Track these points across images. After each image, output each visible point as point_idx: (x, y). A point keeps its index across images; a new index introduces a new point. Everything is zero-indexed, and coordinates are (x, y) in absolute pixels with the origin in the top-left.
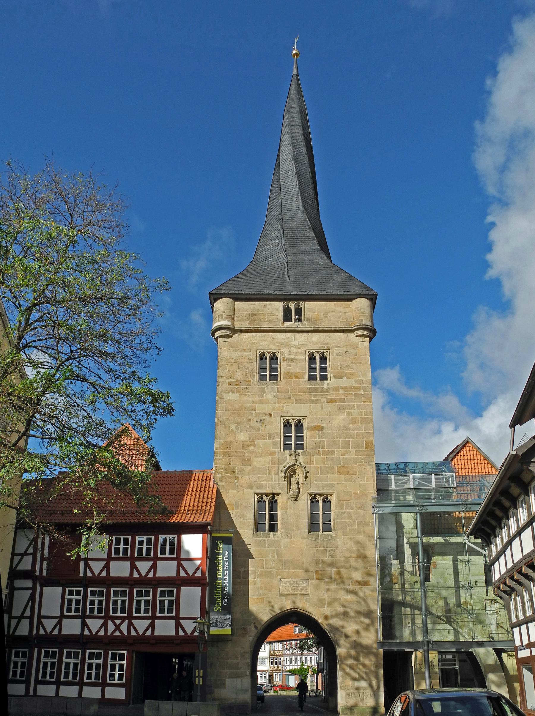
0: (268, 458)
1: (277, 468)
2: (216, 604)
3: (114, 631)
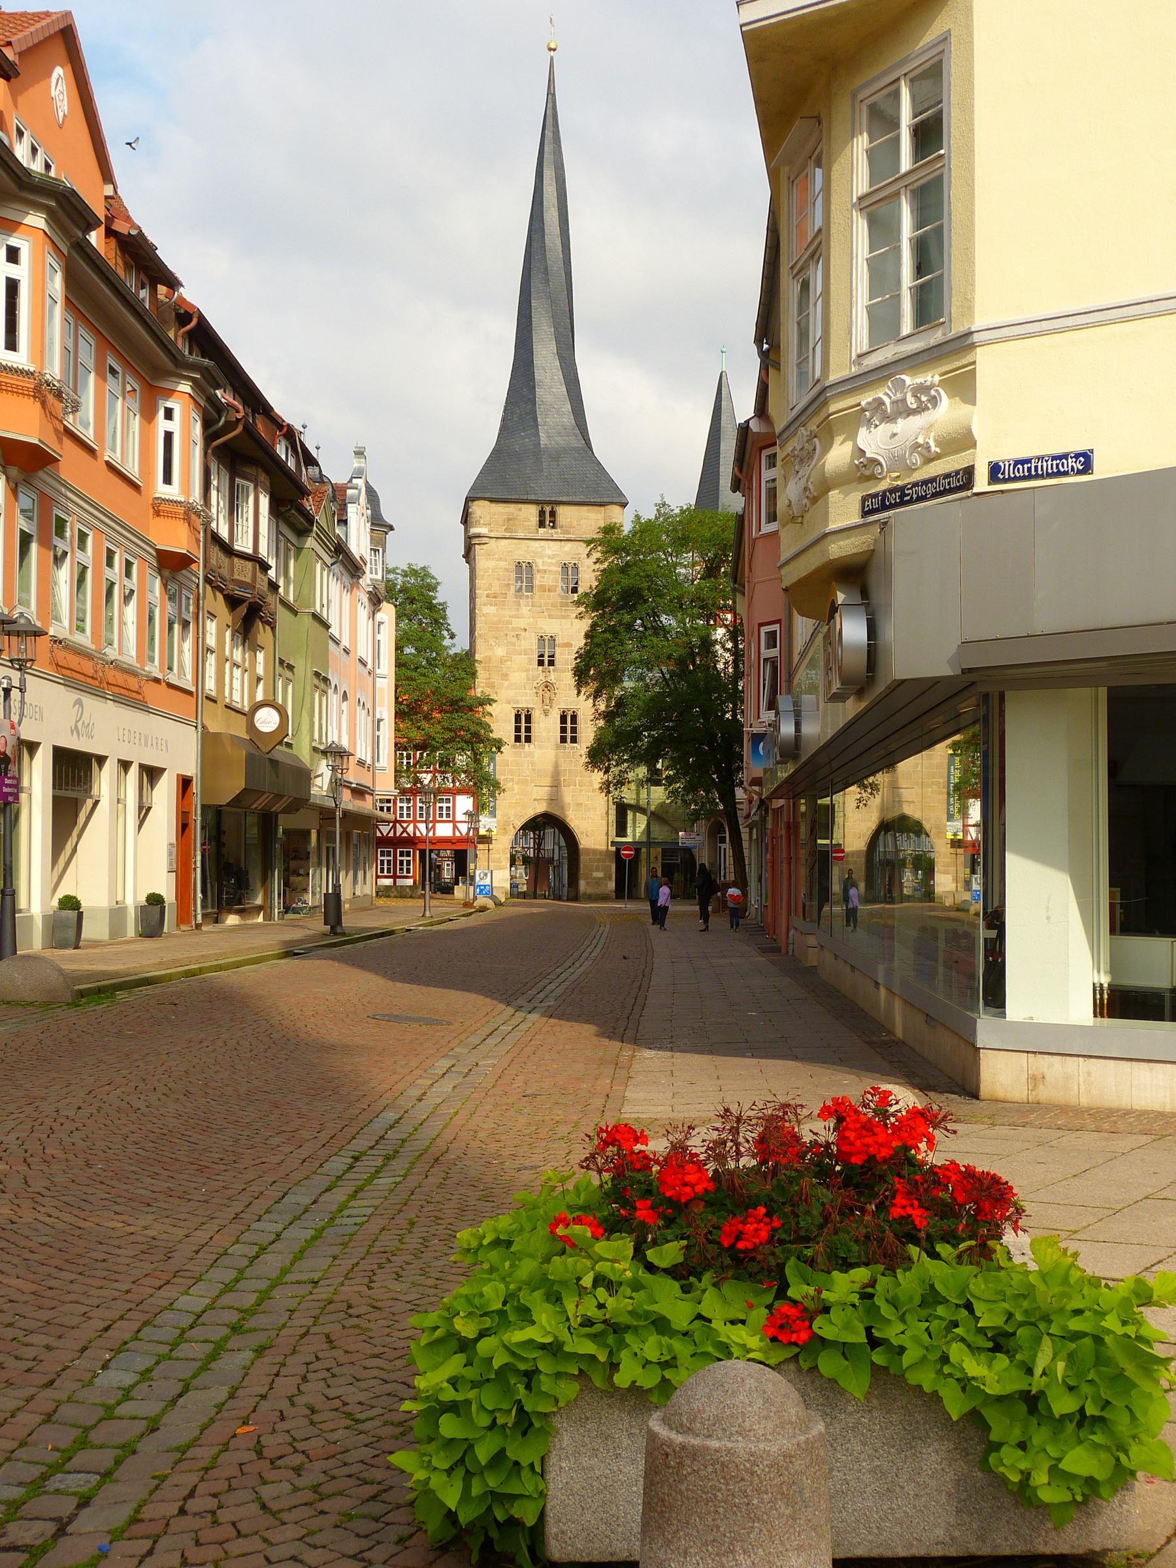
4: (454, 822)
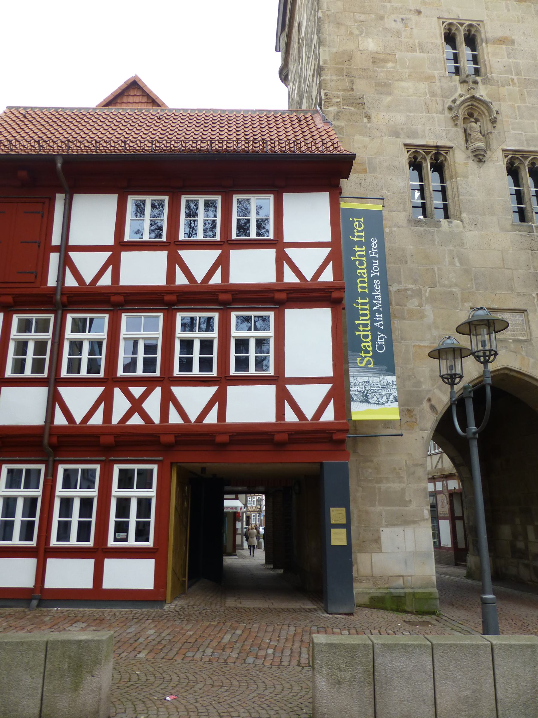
0: (423, 86)
1: (440, 103)
2: (360, 350)
3: (128, 415)
4: (279, 380)
